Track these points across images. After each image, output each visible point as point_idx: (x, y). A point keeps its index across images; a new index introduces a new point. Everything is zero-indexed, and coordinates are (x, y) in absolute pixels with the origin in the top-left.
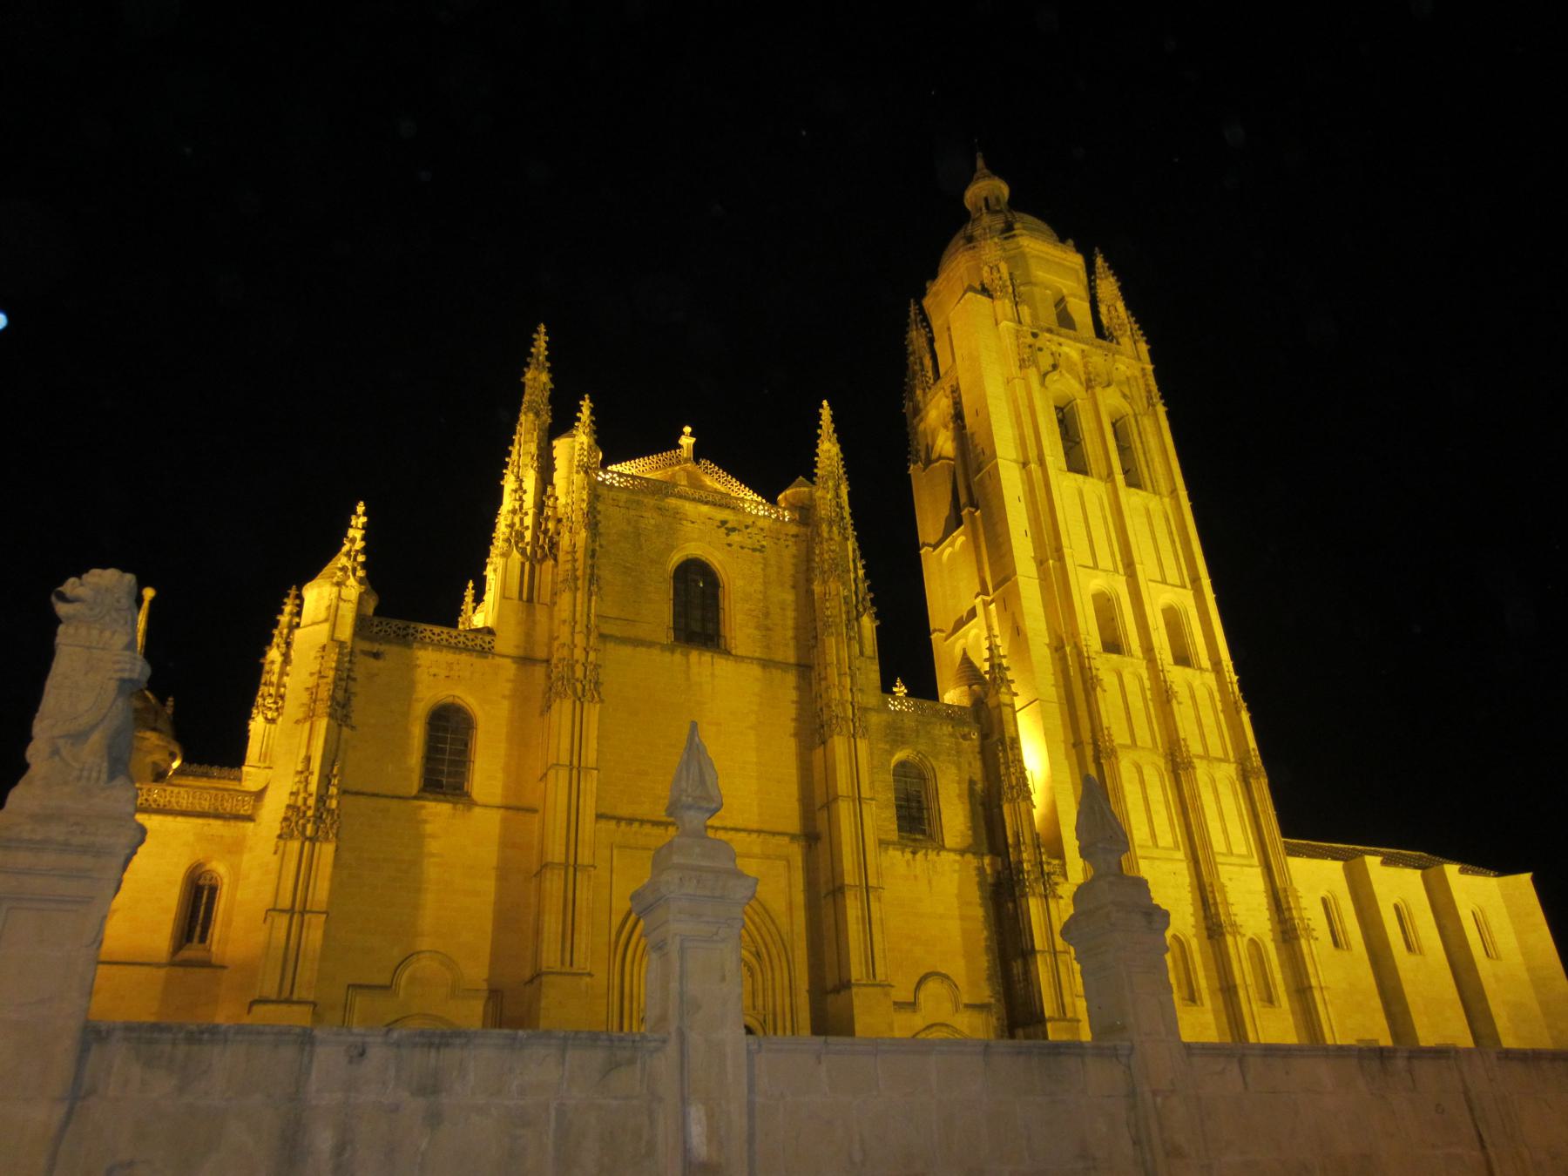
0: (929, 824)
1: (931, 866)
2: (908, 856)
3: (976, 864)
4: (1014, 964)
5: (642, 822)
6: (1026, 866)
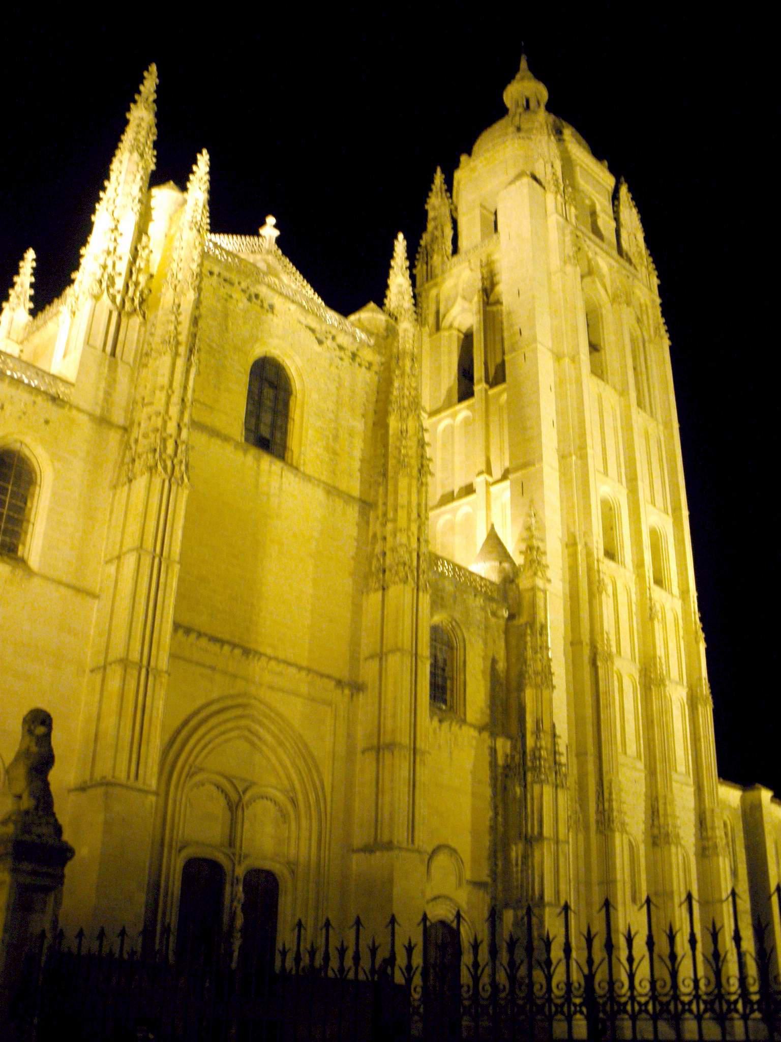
3: (490, 744)
4: (514, 847)
5: (200, 635)
6: (543, 753)
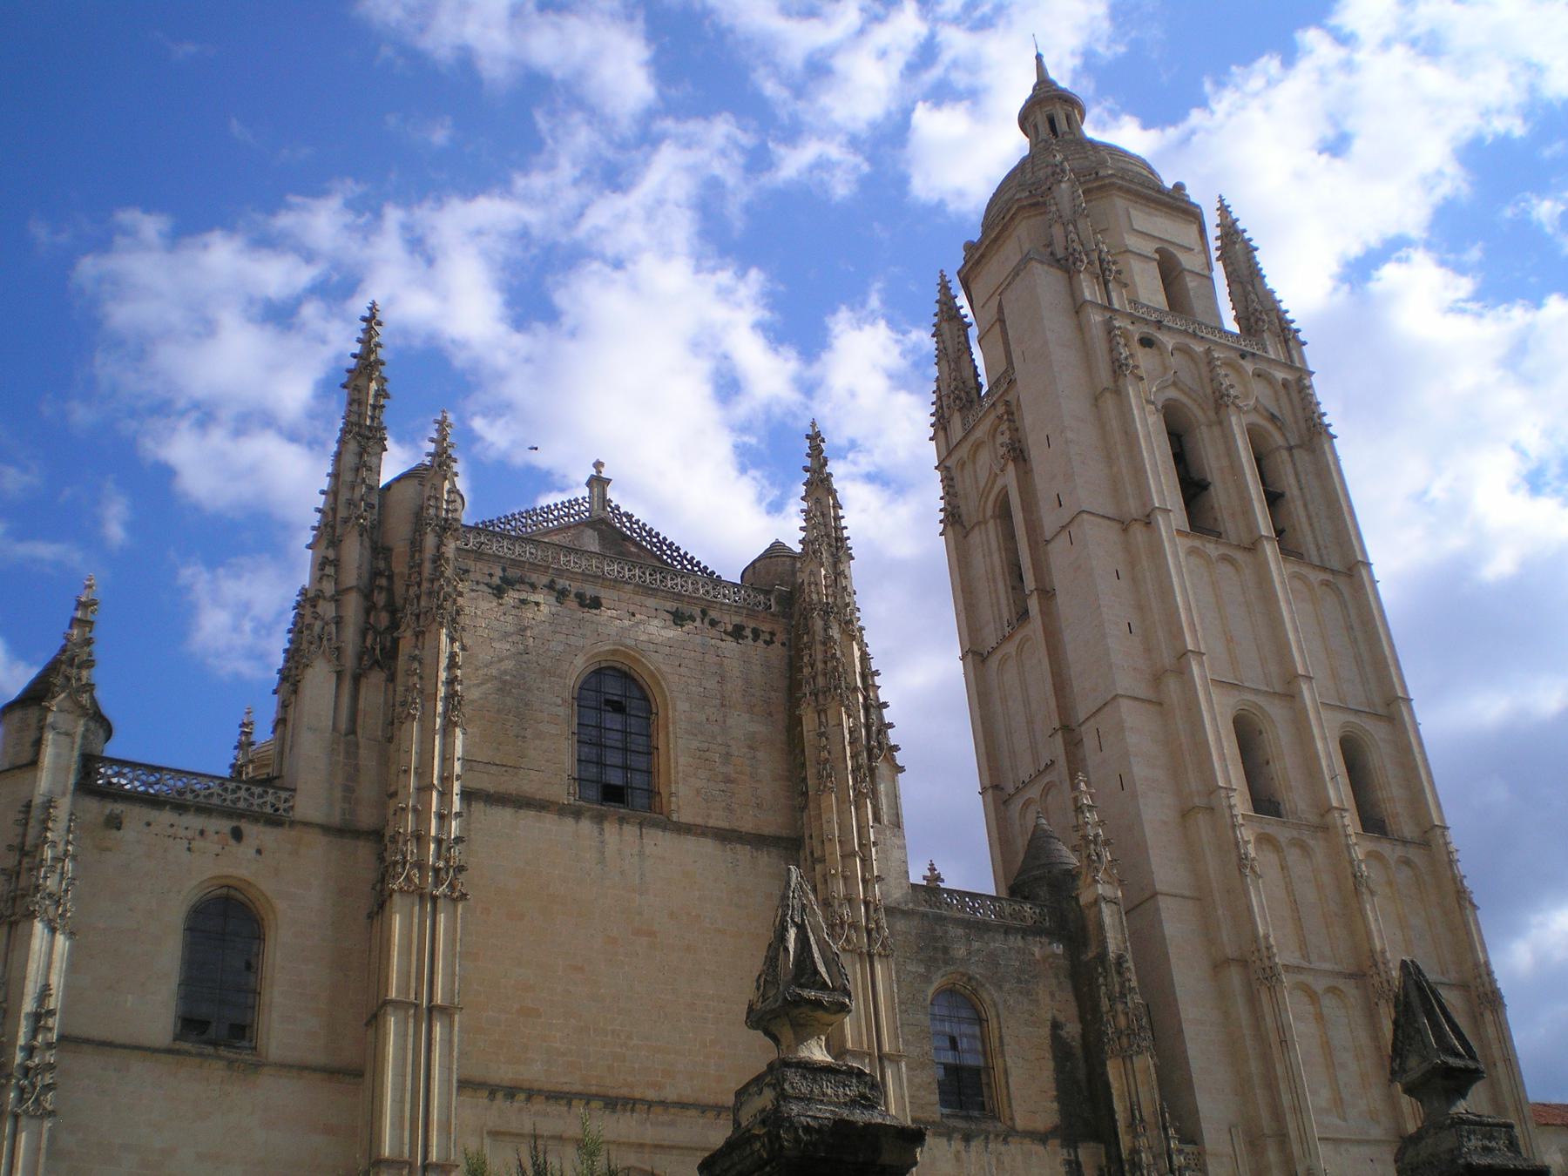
0: (991, 1098)
1: (994, 1162)
2: (958, 1145)
5: (531, 1094)
6: (1145, 1157)
